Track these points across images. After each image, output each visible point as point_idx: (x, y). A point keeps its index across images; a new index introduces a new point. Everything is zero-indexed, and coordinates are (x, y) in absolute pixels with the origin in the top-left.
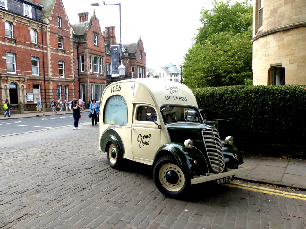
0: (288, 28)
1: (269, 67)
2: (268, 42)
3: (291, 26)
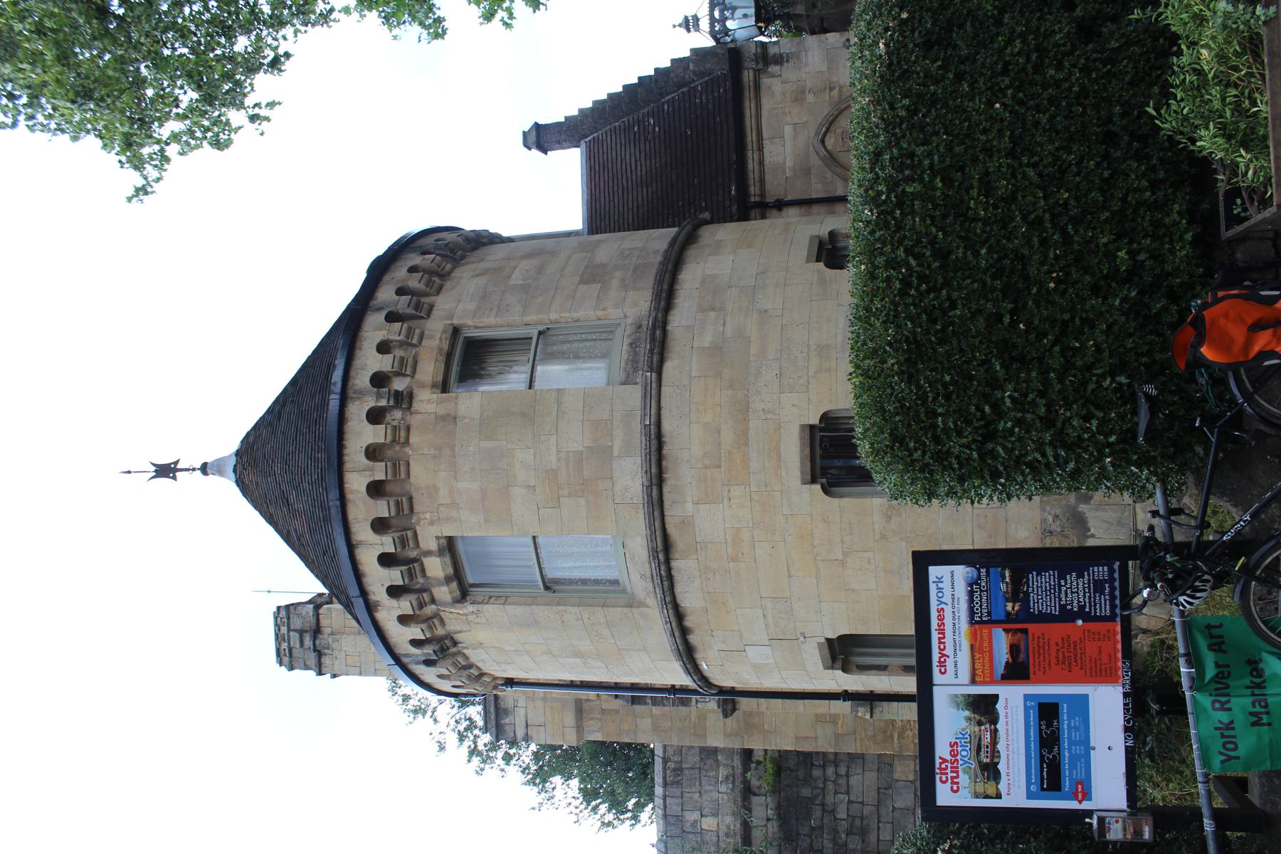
1: (821, 265)
2: (703, 282)
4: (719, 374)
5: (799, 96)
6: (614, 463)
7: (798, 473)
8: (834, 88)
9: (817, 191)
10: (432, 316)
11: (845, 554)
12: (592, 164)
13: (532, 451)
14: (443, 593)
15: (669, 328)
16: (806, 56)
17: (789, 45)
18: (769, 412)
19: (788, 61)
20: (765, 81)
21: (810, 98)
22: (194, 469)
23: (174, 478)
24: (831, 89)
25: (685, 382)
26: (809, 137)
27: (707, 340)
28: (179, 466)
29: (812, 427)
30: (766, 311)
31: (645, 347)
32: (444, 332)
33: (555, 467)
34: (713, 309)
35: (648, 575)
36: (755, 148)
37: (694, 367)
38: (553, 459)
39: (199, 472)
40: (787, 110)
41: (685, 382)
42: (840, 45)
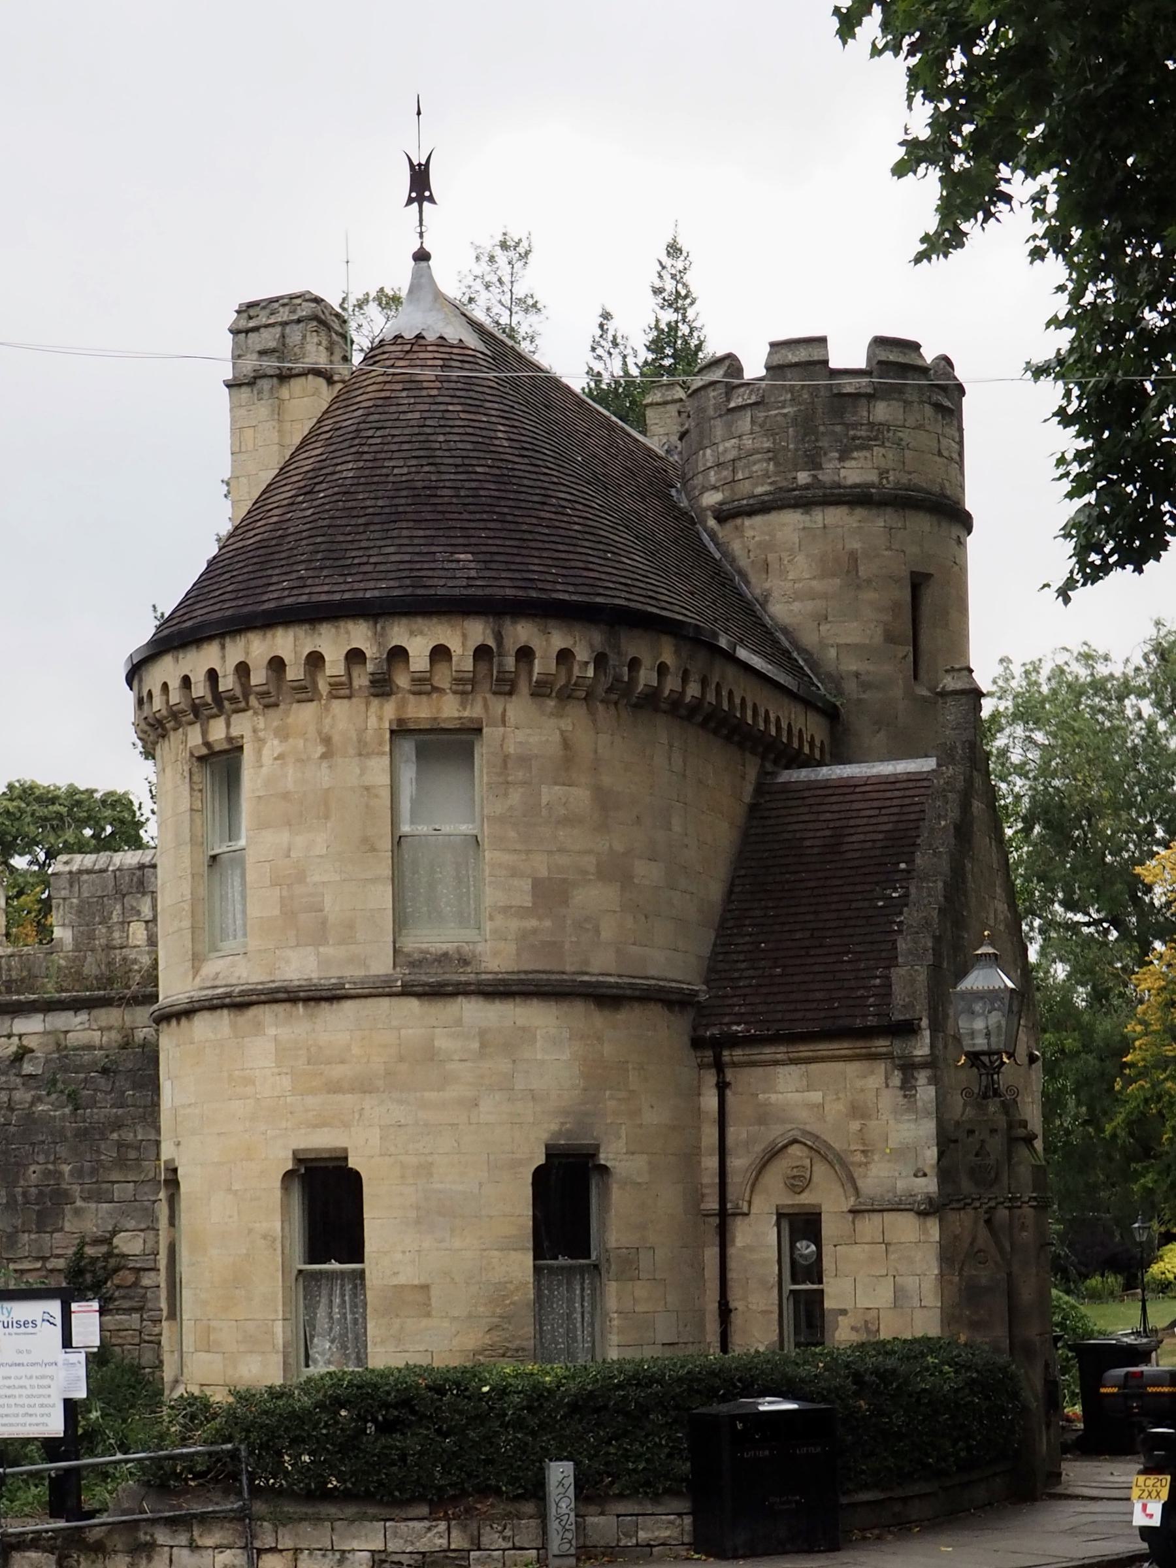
0: (621, 992)
1: (541, 1160)
2: (524, 1029)
4: (401, 1059)
6: (310, 949)
7: (302, 1146)
8: (866, 1157)
11: (236, 1193)
12: (898, 786)
13: (324, 851)
14: (194, 736)
15: (460, 999)
19: (905, 1096)
20: (881, 1067)
21: (855, 1126)
22: (421, 235)
23: (410, 201)
26: (805, 1124)
27: (443, 1042)
28: (426, 204)
29: (346, 1159)
32: (471, 719)
33: (308, 880)
34: (483, 1045)
35: (217, 983)
36: (791, 1055)
37: (410, 1031)
38: (317, 878)
40: (841, 1095)
41: (395, 1023)
42: (920, 1165)
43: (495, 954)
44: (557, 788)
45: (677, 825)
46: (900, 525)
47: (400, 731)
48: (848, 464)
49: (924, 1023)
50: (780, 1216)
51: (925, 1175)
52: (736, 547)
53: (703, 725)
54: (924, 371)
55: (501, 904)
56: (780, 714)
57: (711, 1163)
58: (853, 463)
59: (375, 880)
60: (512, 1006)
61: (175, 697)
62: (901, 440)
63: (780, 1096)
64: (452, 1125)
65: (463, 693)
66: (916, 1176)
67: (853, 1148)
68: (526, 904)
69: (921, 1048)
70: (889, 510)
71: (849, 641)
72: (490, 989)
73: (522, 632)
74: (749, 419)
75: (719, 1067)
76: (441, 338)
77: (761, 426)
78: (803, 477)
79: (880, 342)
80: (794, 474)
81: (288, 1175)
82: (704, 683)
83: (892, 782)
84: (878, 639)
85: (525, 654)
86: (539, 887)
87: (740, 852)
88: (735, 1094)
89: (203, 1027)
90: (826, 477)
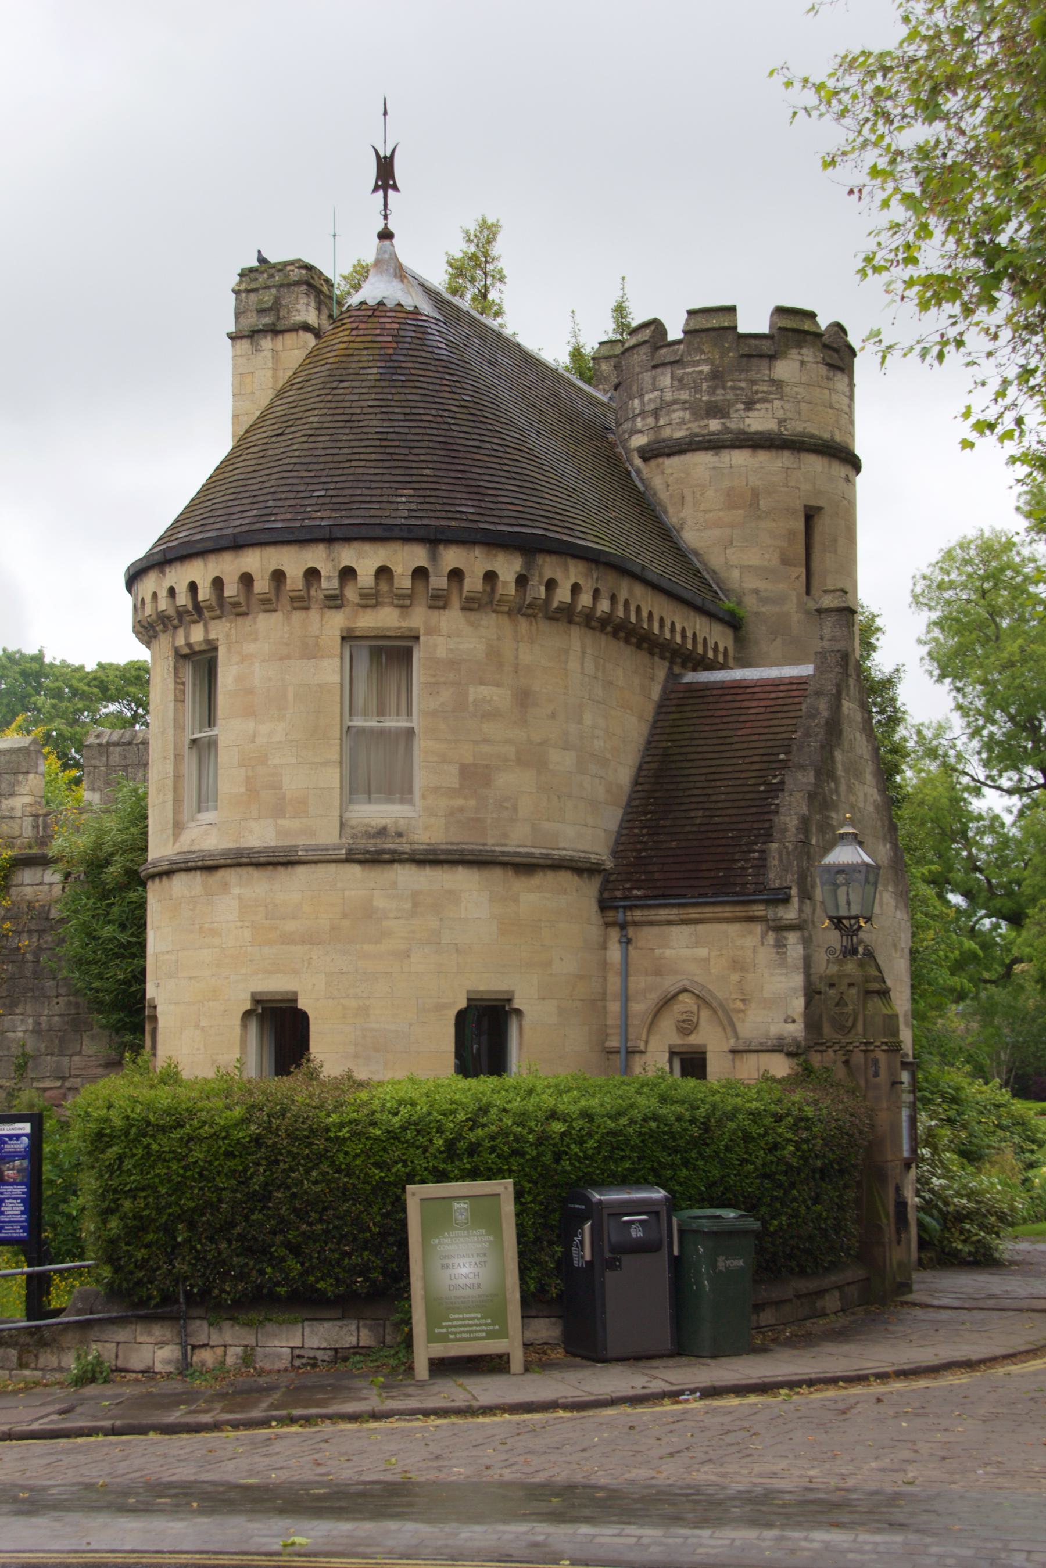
0: (535, 861)
1: (463, 1004)
3: (546, 856)
4: (345, 916)
5: (737, 965)
6: (270, 821)
8: (745, 1004)
9: (638, 982)
10: (430, 611)
12: (782, 688)
13: (283, 739)
15: (396, 866)
16: (781, 974)
17: (795, 955)
18: (309, 964)
19: (778, 953)
20: (758, 928)
21: (735, 977)
22: (386, 217)
23: (376, 189)
24: (743, 1000)
25: (339, 885)
27: (380, 902)
28: (391, 193)
29: (296, 1001)
30: (408, 956)
31: (372, 845)
32: (410, 629)
33: (269, 762)
34: (415, 905)
35: (193, 848)
36: (682, 917)
37: (353, 893)
38: (276, 761)
39: (380, 227)
40: (724, 952)
41: (339, 885)
43: (426, 828)
44: (483, 687)
45: (588, 719)
46: (795, 466)
47: (348, 638)
48: (751, 414)
49: (794, 891)
50: (672, 1054)
51: (794, 1021)
52: (657, 482)
53: (615, 634)
54: (818, 335)
55: (432, 785)
56: (685, 625)
57: (614, 1007)
58: (755, 414)
59: (326, 764)
60: (440, 872)
61: (163, 604)
62: (797, 394)
63: (673, 951)
64: (386, 973)
65: (402, 607)
66: (786, 1022)
67: (734, 996)
68: (453, 786)
69: (790, 913)
70: (786, 454)
71: (750, 563)
72: (422, 857)
73: (452, 557)
74: (669, 375)
75: (623, 926)
76: (399, 305)
77: (680, 380)
78: (714, 425)
79: (780, 311)
80: (706, 422)
81: (247, 1015)
82: (613, 598)
83: (776, 684)
84: (775, 561)
85: (456, 575)
86: (466, 772)
87: (649, 742)
88: (636, 948)
89: (179, 884)
90: (733, 425)
